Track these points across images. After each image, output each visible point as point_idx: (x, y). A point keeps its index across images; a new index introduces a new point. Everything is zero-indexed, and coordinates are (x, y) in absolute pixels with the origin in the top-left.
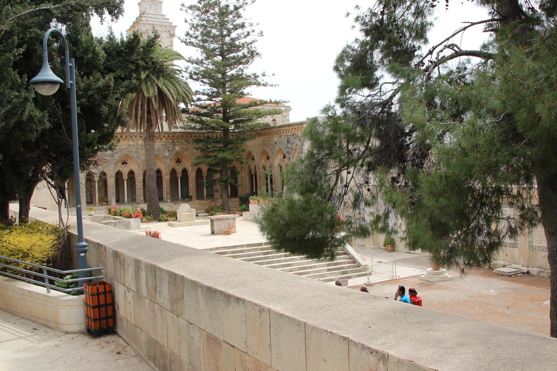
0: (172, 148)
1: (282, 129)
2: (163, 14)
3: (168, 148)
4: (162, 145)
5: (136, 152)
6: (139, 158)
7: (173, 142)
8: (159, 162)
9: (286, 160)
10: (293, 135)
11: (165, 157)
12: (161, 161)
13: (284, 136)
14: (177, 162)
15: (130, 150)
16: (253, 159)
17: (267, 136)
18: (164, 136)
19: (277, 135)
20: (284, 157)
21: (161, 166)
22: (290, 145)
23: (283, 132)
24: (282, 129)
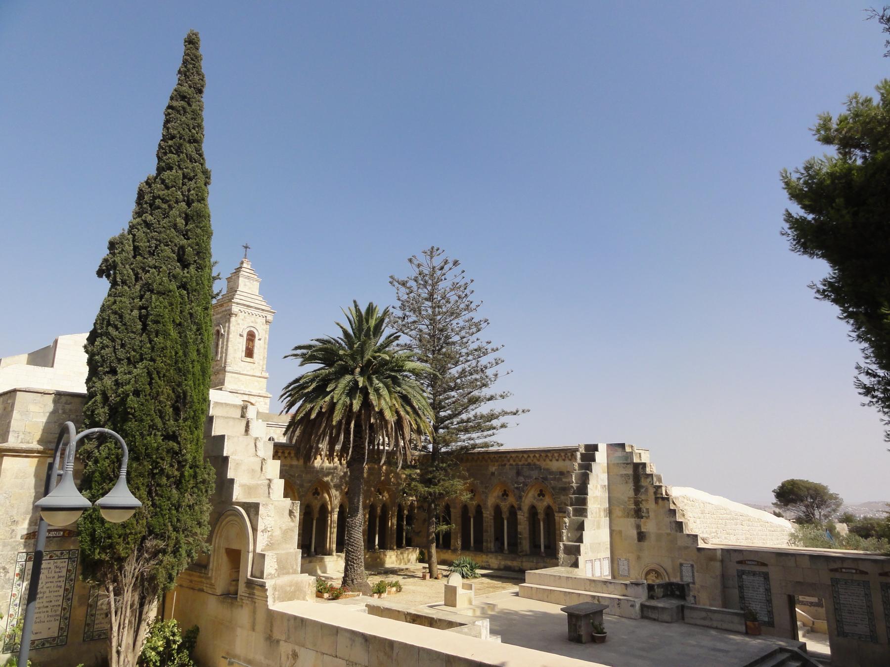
1: (509, 456)
5: (300, 476)
6: (302, 486)
9: (511, 500)
13: (511, 465)
19: (496, 464)
20: (505, 494)
22: (521, 479)
23: (509, 461)
24: (509, 456)
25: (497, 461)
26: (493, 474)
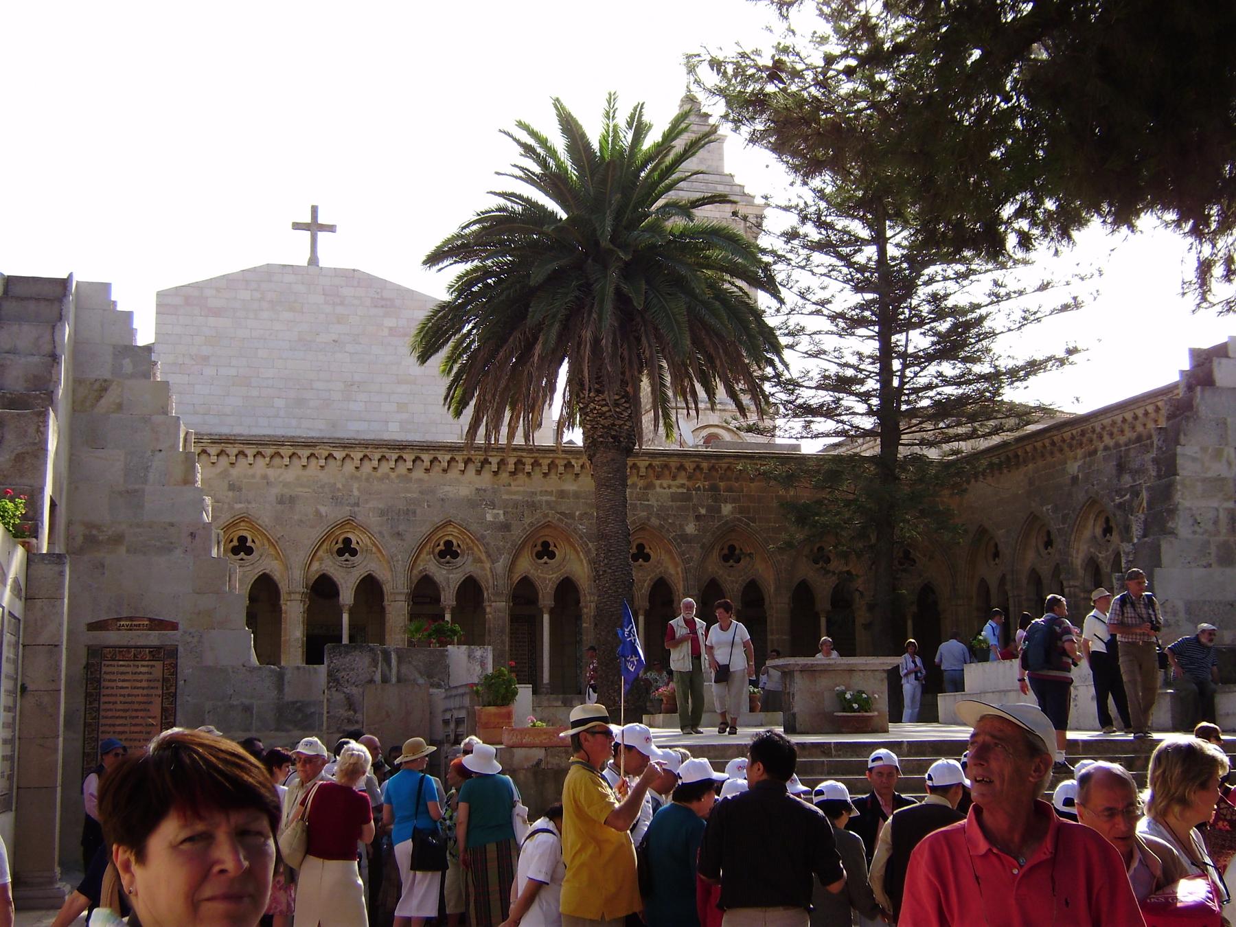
0: (710, 509)
2: (727, 171)
3: (695, 508)
4: (674, 497)
7: (714, 488)
8: (665, 558)
10: (1139, 439)
11: (685, 538)
12: (669, 552)
13: (1106, 448)
14: (726, 558)
15: (563, 509)
16: (996, 555)
17: (1041, 463)
18: (681, 467)
19: (1080, 452)
20: (1107, 530)
21: (672, 571)
22: (1127, 479)
23: (1101, 437)
25: (1081, 445)
26: (1075, 479)
